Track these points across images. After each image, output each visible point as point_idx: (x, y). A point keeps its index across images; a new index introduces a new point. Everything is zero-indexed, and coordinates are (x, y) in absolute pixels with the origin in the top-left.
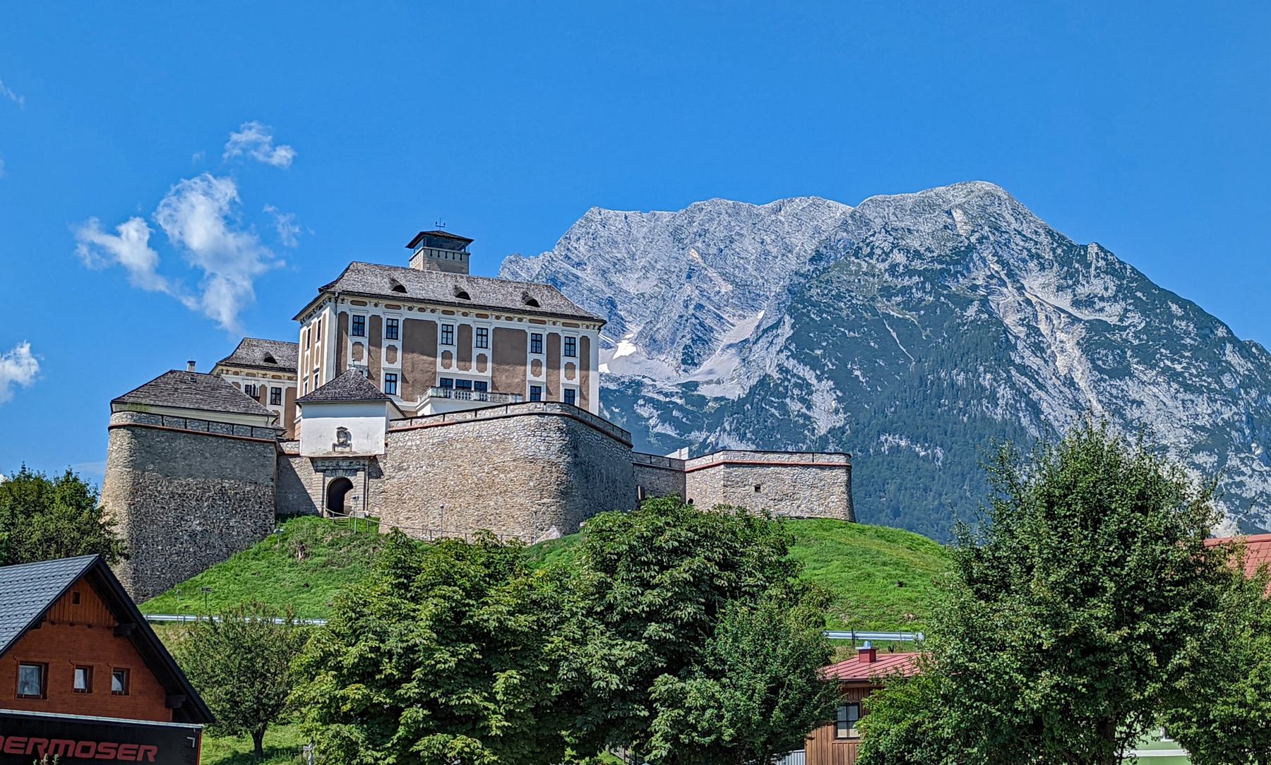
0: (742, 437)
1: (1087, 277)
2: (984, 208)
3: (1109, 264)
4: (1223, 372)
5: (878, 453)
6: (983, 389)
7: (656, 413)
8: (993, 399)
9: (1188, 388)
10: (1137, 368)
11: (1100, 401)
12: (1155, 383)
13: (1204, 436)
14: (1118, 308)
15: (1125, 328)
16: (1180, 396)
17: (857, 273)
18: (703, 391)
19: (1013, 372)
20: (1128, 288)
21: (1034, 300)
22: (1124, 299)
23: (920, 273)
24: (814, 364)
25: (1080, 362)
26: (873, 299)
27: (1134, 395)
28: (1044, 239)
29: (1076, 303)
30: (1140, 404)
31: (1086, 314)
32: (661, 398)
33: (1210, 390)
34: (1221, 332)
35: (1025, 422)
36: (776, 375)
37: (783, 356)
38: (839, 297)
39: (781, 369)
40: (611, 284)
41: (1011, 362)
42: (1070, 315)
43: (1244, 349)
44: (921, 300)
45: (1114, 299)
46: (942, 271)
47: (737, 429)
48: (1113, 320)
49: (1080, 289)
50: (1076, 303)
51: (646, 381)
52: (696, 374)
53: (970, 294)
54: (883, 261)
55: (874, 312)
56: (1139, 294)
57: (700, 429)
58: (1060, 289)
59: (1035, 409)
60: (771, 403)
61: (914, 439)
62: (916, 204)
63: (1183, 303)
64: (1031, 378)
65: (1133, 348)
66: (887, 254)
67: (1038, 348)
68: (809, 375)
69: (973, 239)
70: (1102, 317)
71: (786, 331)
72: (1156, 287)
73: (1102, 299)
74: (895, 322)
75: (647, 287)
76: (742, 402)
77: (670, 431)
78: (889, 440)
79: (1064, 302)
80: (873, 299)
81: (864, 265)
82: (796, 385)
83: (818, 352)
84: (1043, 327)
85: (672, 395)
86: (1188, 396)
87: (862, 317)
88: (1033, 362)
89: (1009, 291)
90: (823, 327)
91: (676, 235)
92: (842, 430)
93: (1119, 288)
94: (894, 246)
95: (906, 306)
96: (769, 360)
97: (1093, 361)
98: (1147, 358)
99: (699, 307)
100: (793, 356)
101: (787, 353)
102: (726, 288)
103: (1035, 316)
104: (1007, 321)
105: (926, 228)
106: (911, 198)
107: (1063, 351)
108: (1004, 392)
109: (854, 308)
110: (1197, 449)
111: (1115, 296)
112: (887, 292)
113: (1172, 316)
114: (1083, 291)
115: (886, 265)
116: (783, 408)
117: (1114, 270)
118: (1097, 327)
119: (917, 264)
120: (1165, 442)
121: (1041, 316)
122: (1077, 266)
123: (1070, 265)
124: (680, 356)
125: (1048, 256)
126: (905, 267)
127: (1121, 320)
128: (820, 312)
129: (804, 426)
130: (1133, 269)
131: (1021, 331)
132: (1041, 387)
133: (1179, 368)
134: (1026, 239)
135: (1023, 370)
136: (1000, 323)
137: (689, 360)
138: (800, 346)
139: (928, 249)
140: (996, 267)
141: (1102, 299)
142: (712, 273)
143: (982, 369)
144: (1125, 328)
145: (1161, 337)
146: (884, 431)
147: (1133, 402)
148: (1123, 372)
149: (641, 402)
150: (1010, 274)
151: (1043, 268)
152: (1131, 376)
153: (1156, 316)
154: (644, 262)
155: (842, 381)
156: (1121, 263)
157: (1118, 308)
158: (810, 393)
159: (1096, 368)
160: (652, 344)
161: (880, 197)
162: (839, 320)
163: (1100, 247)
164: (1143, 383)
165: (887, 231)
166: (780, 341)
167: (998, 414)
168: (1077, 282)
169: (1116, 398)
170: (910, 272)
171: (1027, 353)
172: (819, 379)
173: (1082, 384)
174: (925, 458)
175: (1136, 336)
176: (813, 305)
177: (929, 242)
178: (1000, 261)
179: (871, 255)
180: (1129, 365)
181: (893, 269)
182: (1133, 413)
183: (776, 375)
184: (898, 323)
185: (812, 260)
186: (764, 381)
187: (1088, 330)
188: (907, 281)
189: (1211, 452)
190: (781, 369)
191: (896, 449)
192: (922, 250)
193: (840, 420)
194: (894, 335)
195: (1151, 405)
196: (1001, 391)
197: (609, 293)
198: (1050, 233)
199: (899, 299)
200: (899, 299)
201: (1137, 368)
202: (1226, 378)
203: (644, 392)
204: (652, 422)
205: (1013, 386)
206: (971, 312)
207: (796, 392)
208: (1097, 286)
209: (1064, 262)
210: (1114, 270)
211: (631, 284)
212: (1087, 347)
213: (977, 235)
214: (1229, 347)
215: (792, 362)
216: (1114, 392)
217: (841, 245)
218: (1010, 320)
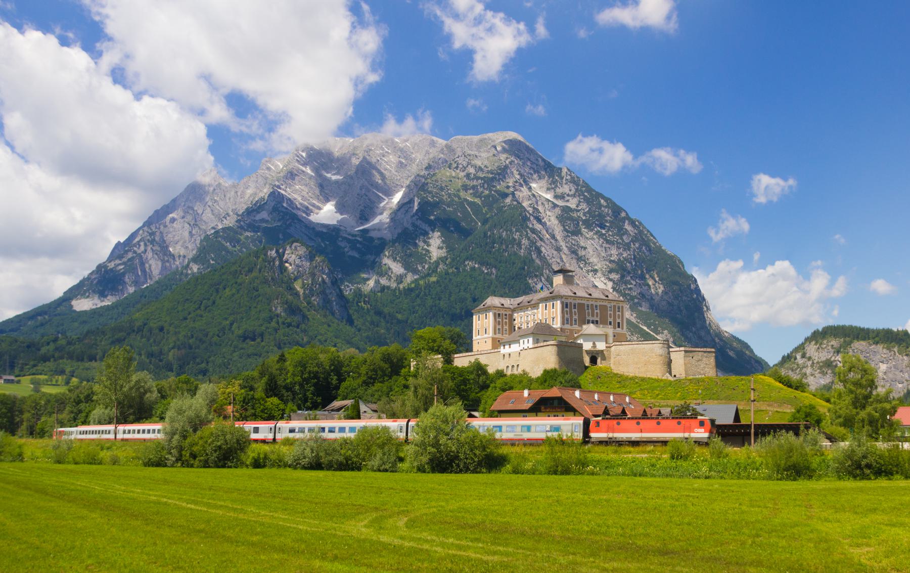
0: (395, 260)
1: (561, 184)
3: (572, 178)
4: (623, 234)
5: (464, 270)
6: (514, 239)
7: (348, 245)
8: (519, 245)
9: (608, 242)
10: (584, 230)
11: (567, 247)
12: (593, 239)
15: (578, 211)
16: (604, 245)
21: (536, 194)
22: (579, 196)
23: (482, 179)
25: (557, 227)
26: (459, 191)
27: (582, 244)
30: (585, 248)
31: (560, 203)
32: (350, 237)
33: (618, 243)
34: (623, 215)
35: (534, 256)
36: (411, 228)
37: (414, 218)
41: (528, 227)
42: (553, 203)
43: (633, 223)
44: (482, 192)
45: (574, 196)
47: (392, 255)
48: (573, 206)
51: (342, 228)
53: (506, 191)
54: (463, 171)
55: (459, 197)
56: (586, 194)
58: (548, 189)
59: (539, 251)
61: (482, 263)
63: (606, 199)
64: (537, 235)
66: (465, 168)
67: (539, 220)
69: (507, 162)
70: (568, 204)
72: (594, 191)
73: (568, 195)
78: (470, 264)
79: (549, 196)
80: (459, 191)
84: (540, 208)
85: (356, 236)
86: (608, 246)
87: (453, 200)
89: (524, 189)
93: (577, 190)
94: (469, 164)
95: (475, 195)
97: (564, 227)
98: (588, 225)
101: (416, 217)
103: (537, 203)
105: (484, 155)
106: (476, 138)
108: (525, 242)
109: (449, 195)
110: (611, 271)
111: (575, 194)
113: (601, 206)
114: (559, 191)
117: (574, 181)
118: (566, 210)
119: (481, 175)
120: (596, 267)
121: (540, 203)
122: (557, 178)
123: (553, 177)
124: (358, 215)
126: (474, 175)
127: (577, 206)
128: (433, 197)
129: (425, 255)
130: (583, 181)
132: (541, 239)
133: (604, 232)
135: (534, 231)
139: (485, 166)
141: (568, 195)
143: (514, 230)
144: (578, 211)
146: (467, 259)
147: (582, 247)
148: (577, 232)
149: (340, 239)
150: (525, 181)
151: (540, 178)
153: (594, 205)
156: (577, 177)
159: (565, 230)
160: (340, 208)
163: (569, 170)
164: (587, 238)
165: (465, 156)
168: (557, 186)
169: (574, 245)
170: (478, 178)
173: (558, 238)
175: (584, 214)
177: (486, 162)
179: (457, 168)
180: (580, 229)
182: (581, 253)
183: (411, 228)
184: (471, 204)
185: (426, 168)
188: (475, 183)
189: (617, 273)
190: (413, 225)
191: (473, 269)
192: (483, 167)
193: (443, 253)
194: (469, 210)
195: (590, 250)
196: (523, 241)
199: (471, 191)
200: (471, 191)
201: (584, 230)
202: (625, 237)
204: (346, 250)
205: (529, 239)
206: (508, 200)
208: (566, 189)
210: (574, 181)
212: (562, 219)
213: (509, 160)
214: (627, 222)
216: (573, 242)
217: (440, 161)
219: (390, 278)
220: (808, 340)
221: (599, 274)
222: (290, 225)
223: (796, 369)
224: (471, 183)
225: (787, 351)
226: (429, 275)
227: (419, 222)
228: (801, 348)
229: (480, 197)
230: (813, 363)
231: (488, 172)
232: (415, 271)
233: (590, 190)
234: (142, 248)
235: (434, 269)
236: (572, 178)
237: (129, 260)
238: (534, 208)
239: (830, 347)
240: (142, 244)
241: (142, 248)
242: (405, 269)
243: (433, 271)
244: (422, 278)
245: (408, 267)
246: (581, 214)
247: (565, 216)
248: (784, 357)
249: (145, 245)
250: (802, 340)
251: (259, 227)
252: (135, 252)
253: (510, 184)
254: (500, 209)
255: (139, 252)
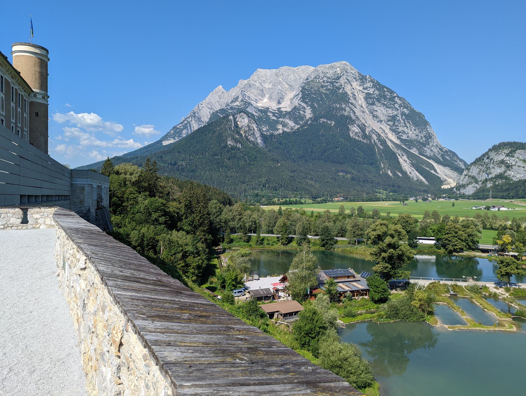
0: (290, 120)
1: (366, 83)
2: (344, 67)
3: (371, 80)
4: (395, 104)
5: (320, 123)
6: (343, 108)
7: (272, 115)
8: (345, 110)
9: (387, 107)
10: (376, 103)
12: (380, 106)
13: (391, 118)
14: (373, 90)
15: (374, 94)
17: (316, 83)
18: (282, 109)
19: (350, 104)
20: (375, 85)
23: (330, 82)
24: (306, 103)
27: (375, 109)
28: (357, 74)
29: (364, 89)
30: (377, 111)
31: (366, 91)
33: (392, 108)
35: (352, 115)
36: (298, 106)
37: (299, 101)
38: (312, 88)
39: (299, 104)
40: (262, 86)
41: (349, 102)
42: (362, 91)
43: (400, 98)
44: (330, 88)
45: (372, 88)
46: (334, 82)
48: (372, 93)
49: (365, 86)
50: (364, 89)
51: (270, 108)
52: (280, 106)
53: (340, 87)
55: (319, 91)
57: (281, 118)
58: (360, 85)
59: (354, 113)
60: (296, 112)
62: (329, 67)
63: (387, 88)
64: (353, 105)
65: (376, 99)
67: (355, 99)
68: (305, 106)
69: (341, 74)
70: (369, 92)
71: (300, 96)
73: (369, 88)
74: (324, 93)
75: (270, 86)
76: (290, 112)
77: (274, 118)
79: (361, 88)
81: (317, 81)
82: (302, 108)
83: (307, 100)
84: (356, 94)
86: (387, 109)
88: (354, 102)
89: (349, 86)
90: (308, 95)
91: (277, 75)
92: (312, 118)
93: (373, 85)
94: (324, 76)
95: (327, 90)
96: (296, 102)
97: (367, 102)
98: (379, 100)
99: (282, 91)
100: (302, 101)
102: (287, 86)
104: (348, 93)
105: (331, 72)
106: (328, 66)
107: (360, 99)
108: (348, 109)
109: (315, 90)
110: (389, 121)
112: (322, 86)
113: (385, 91)
115: (322, 80)
116: (299, 113)
118: (368, 94)
119: (329, 80)
121: (356, 92)
125: (358, 78)
128: (308, 91)
129: (304, 117)
131: (352, 95)
132: (355, 107)
133: (386, 103)
134: (353, 74)
135: (352, 104)
136: (347, 93)
137: (279, 103)
138: (303, 99)
139: (332, 77)
140: (346, 81)
141: (369, 88)
142: (284, 83)
144: (374, 94)
145: (382, 96)
146: (321, 118)
147: (375, 111)
148: (373, 104)
150: (349, 82)
151: (357, 81)
152: (375, 105)
154: (269, 81)
155: (312, 107)
157: (373, 90)
158: (305, 110)
159: (368, 103)
161: (321, 65)
162: (312, 93)
163: (370, 76)
166: (299, 98)
167: (346, 114)
170: (328, 82)
171: (353, 100)
172: (307, 106)
173: (364, 107)
174: (330, 124)
176: (306, 90)
178: (347, 79)
181: (324, 81)
182: (375, 113)
185: (306, 80)
186: (295, 107)
187: (366, 95)
189: (392, 121)
190: (299, 104)
191: (324, 122)
193: (311, 116)
195: (379, 111)
196: (347, 108)
197: (262, 88)
198: (358, 73)
199: (325, 88)
200: (325, 88)
201: (376, 103)
202: (396, 105)
203: (269, 110)
204: (271, 116)
205: (350, 107)
206: (341, 91)
207: (302, 109)
208: (369, 85)
209: (361, 79)
211: (267, 86)
212: (366, 99)
214: (396, 98)
215: (301, 103)
218: (349, 93)
219: (288, 128)
220: (490, 150)
221: (383, 122)
222: (248, 107)
223: (484, 165)
224: (325, 84)
225: (478, 155)
226: (304, 126)
227: (301, 103)
228: (487, 153)
229: (329, 90)
230: (494, 162)
231: (333, 79)
232: (299, 124)
233: (379, 84)
234: (190, 119)
235: (306, 124)
236: (371, 80)
237: (185, 124)
238: (353, 94)
239: (503, 153)
240: (190, 117)
241: (190, 119)
242: (295, 123)
243: (306, 124)
244: (301, 127)
245: (296, 123)
246: (375, 96)
247: (368, 96)
248: (476, 159)
249: (192, 118)
250: (487, 150)
251: (235, 108)
252: (188, 121)
253: (343, 84)
254: (337, 95)
255: (189, 121)
